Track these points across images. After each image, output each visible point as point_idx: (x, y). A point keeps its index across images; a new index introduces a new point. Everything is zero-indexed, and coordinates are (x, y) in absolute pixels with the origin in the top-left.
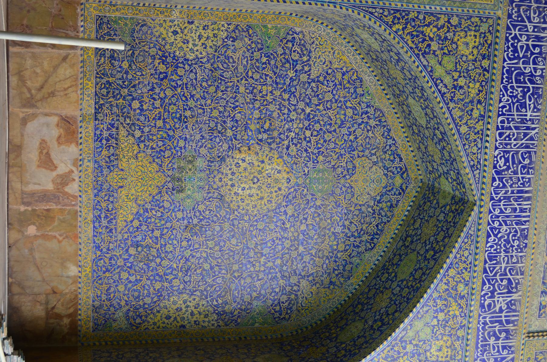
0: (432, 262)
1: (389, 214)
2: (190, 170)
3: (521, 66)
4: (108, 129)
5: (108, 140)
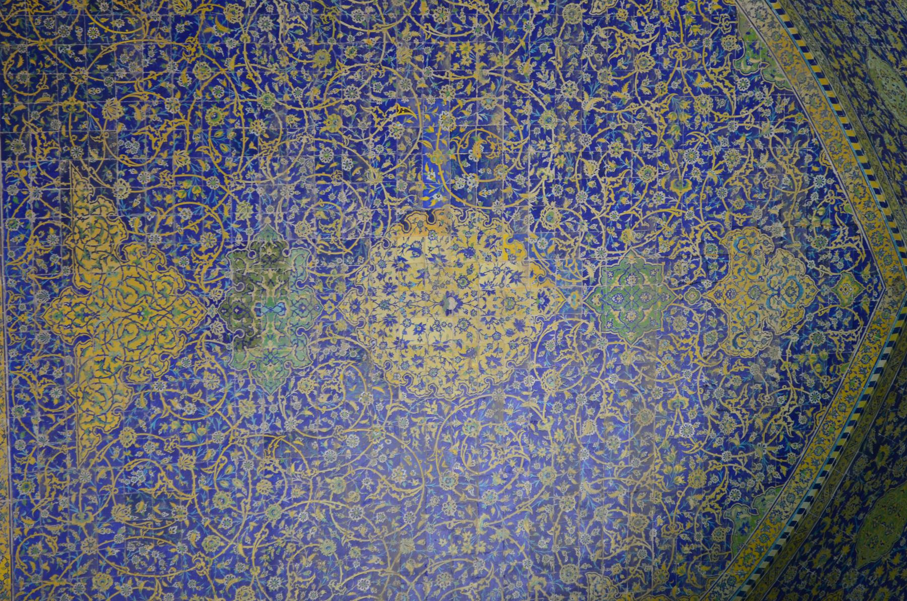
1: (825, 381)
2: (271, 282)
4: (41, 180)
5: (40, 211)
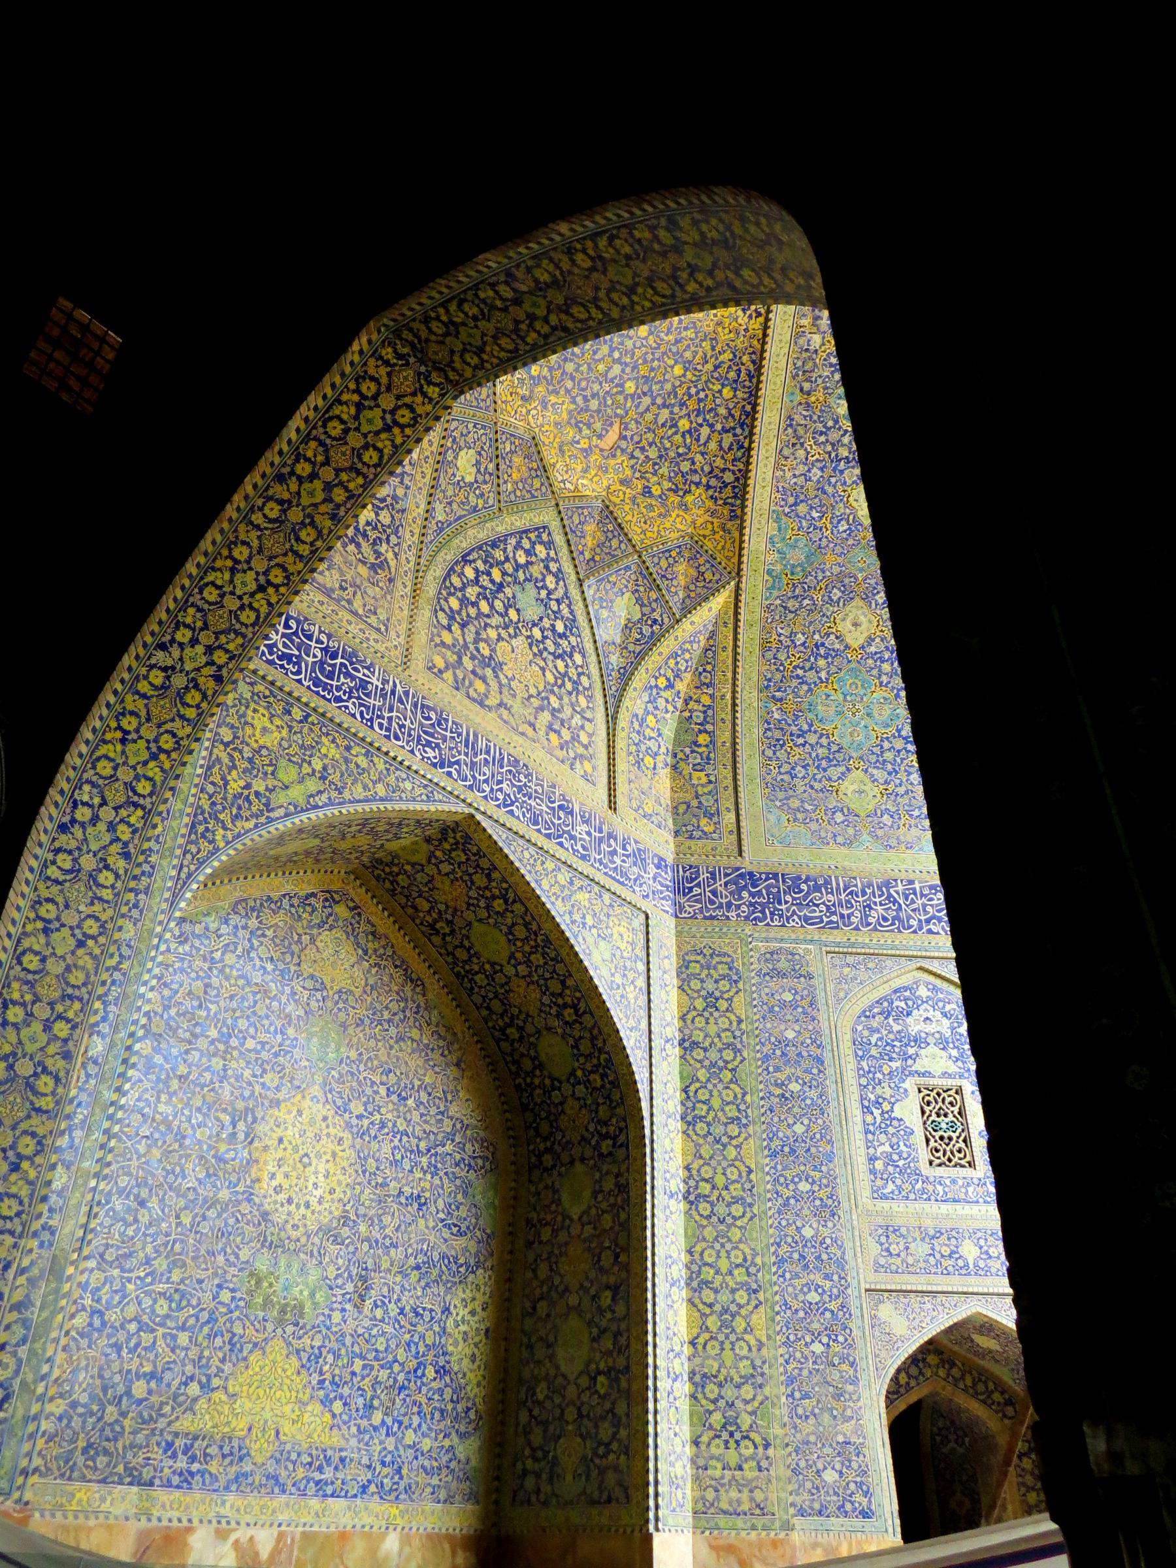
0: (518, 908)
2: (271, 1285)
3: (311, 660)
4: (174, 1456)
5: (193, 1459)
